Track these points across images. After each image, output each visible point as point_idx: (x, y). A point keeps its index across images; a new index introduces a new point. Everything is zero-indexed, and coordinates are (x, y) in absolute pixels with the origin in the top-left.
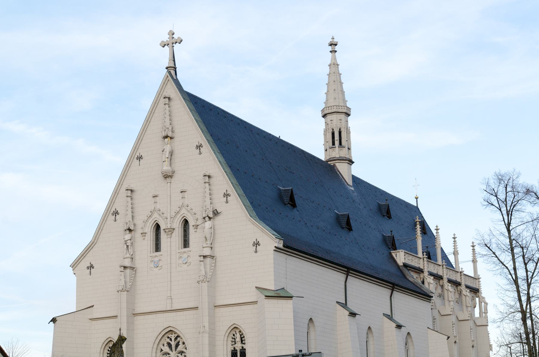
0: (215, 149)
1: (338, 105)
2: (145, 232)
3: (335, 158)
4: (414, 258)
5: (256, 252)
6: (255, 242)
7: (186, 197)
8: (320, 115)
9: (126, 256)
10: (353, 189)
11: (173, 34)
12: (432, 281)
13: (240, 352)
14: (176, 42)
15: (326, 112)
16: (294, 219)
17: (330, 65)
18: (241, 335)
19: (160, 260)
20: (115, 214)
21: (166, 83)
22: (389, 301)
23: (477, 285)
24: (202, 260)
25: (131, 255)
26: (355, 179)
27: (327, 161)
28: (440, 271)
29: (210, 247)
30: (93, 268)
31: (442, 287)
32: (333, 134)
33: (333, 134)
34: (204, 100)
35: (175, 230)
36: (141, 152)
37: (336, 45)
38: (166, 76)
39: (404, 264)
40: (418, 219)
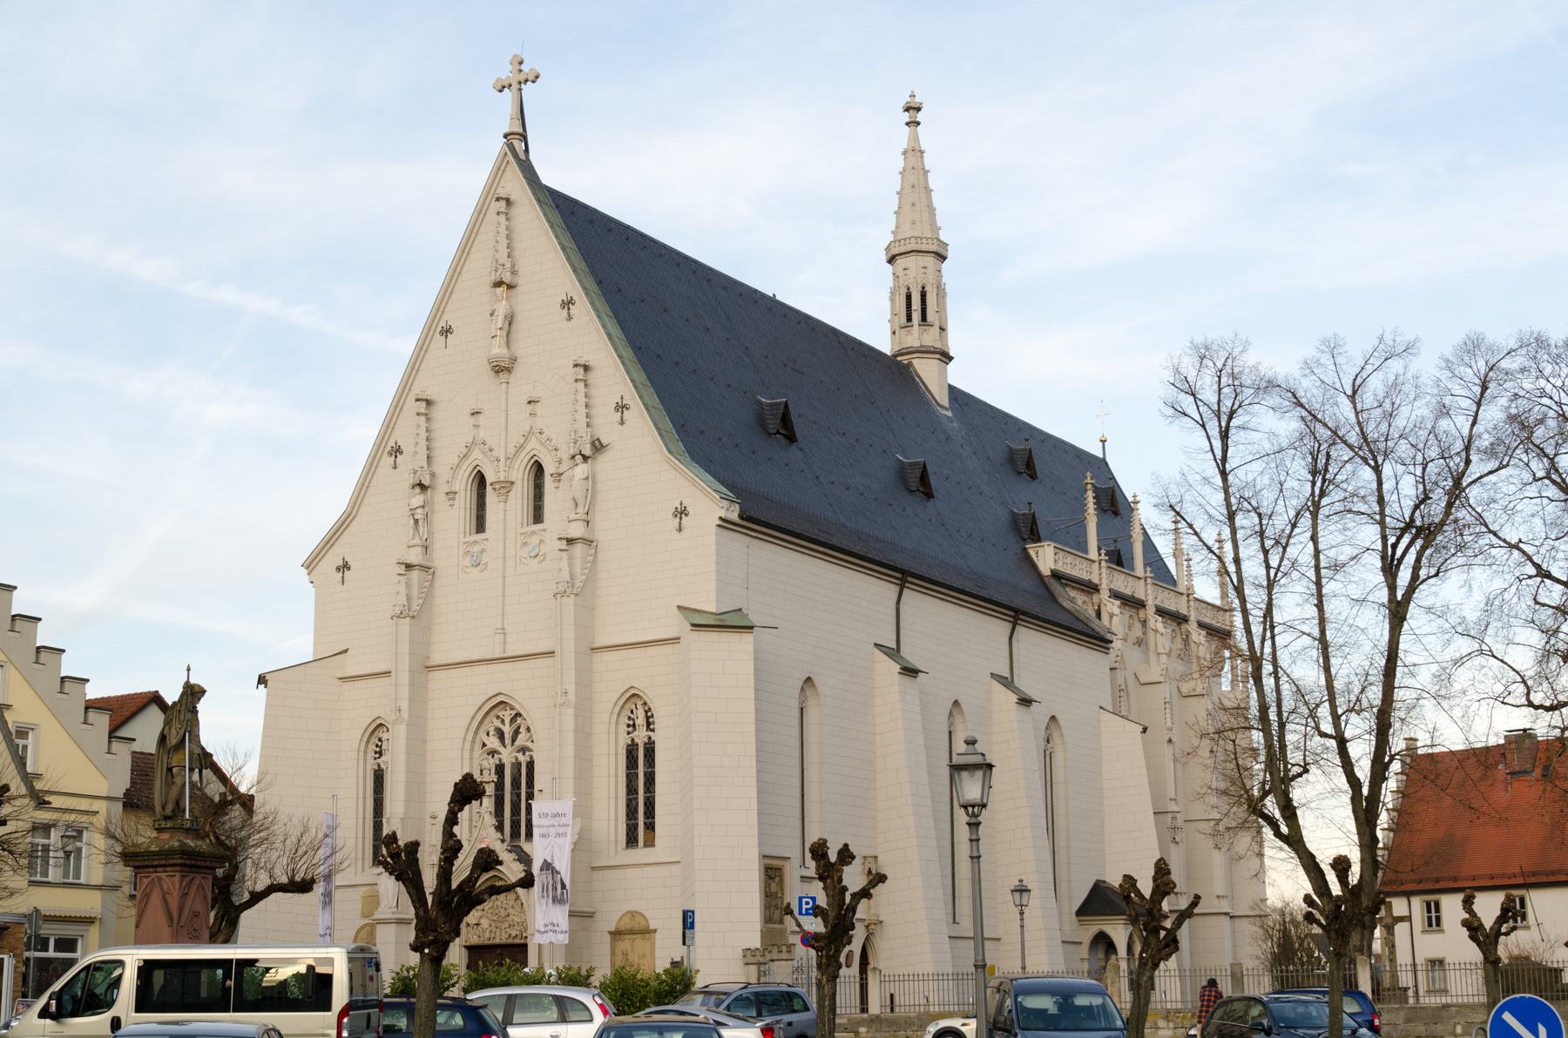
0: (600, 308)
1: (920, 235)
2: (453, 490)
3: (912, 349)
4: (1078, 560)
5: (680, 530)
6: (679, 509)
7: (539, 413)
8: (884, 258)
9: (412, 543)
10: (949, 414)
11: (521, 63)
12: (1116, 610)
13: (645, 748)
14: (526, 81)
15: (895, 251)
16: (787, 465)
17: (905, 153)
18: (646, 712)
19: (483, 551)
21: (503, 168)
22: (1007, 647)
23: (1228, 623)
24: (564, 547)
25: (424, 539)
26: (954, 392)
27: (895, 356)
28: (1139, 590)
29: (584, 520)
30: (349, 569)
31: (1144, 623)
32: (909, 297)
33: (909, 297)
34: (595, 209)
35: (514, 486)
36: (450, 318)
37: (918, 109)
38: (503, 153)
39: (1052, 571)
40: (1089, 478)
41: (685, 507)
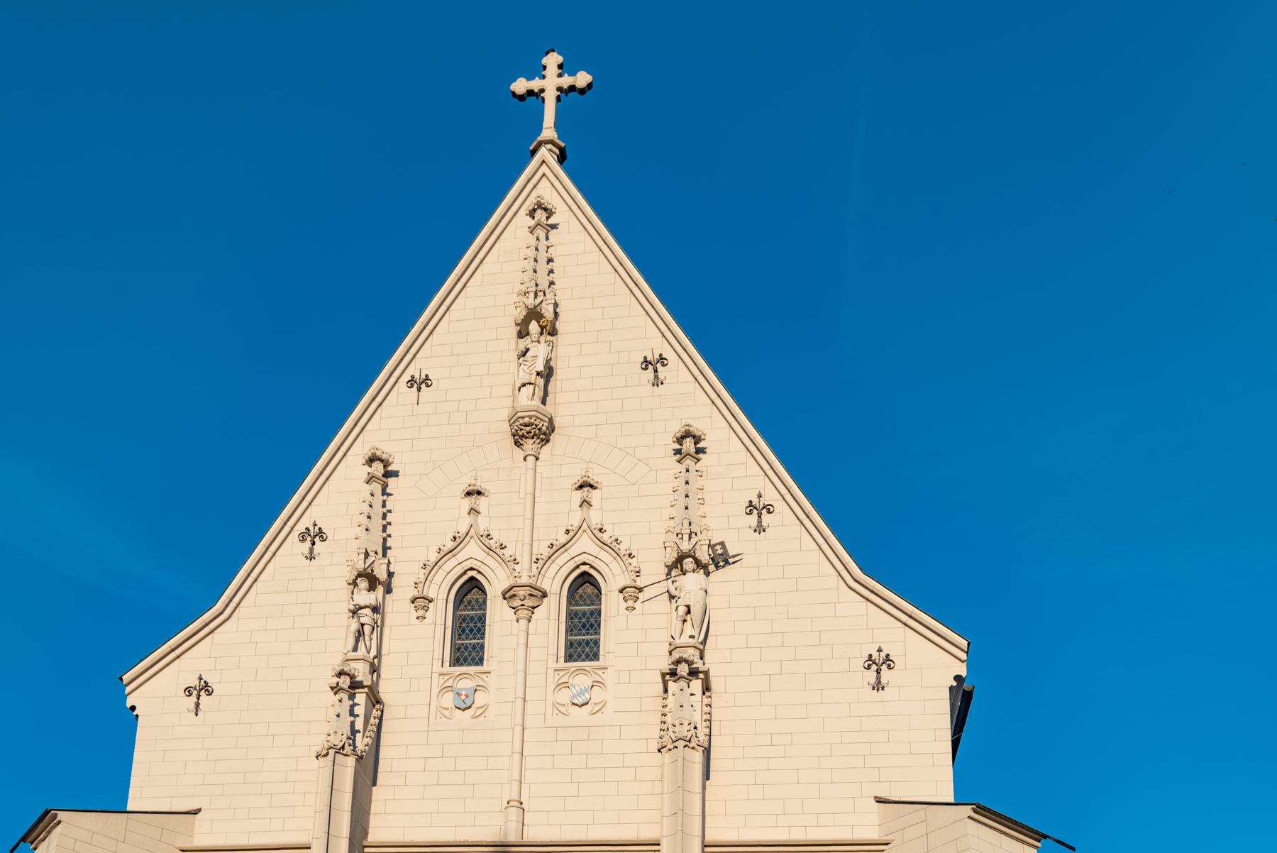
20: (309, 539)
41: (888, 655)
